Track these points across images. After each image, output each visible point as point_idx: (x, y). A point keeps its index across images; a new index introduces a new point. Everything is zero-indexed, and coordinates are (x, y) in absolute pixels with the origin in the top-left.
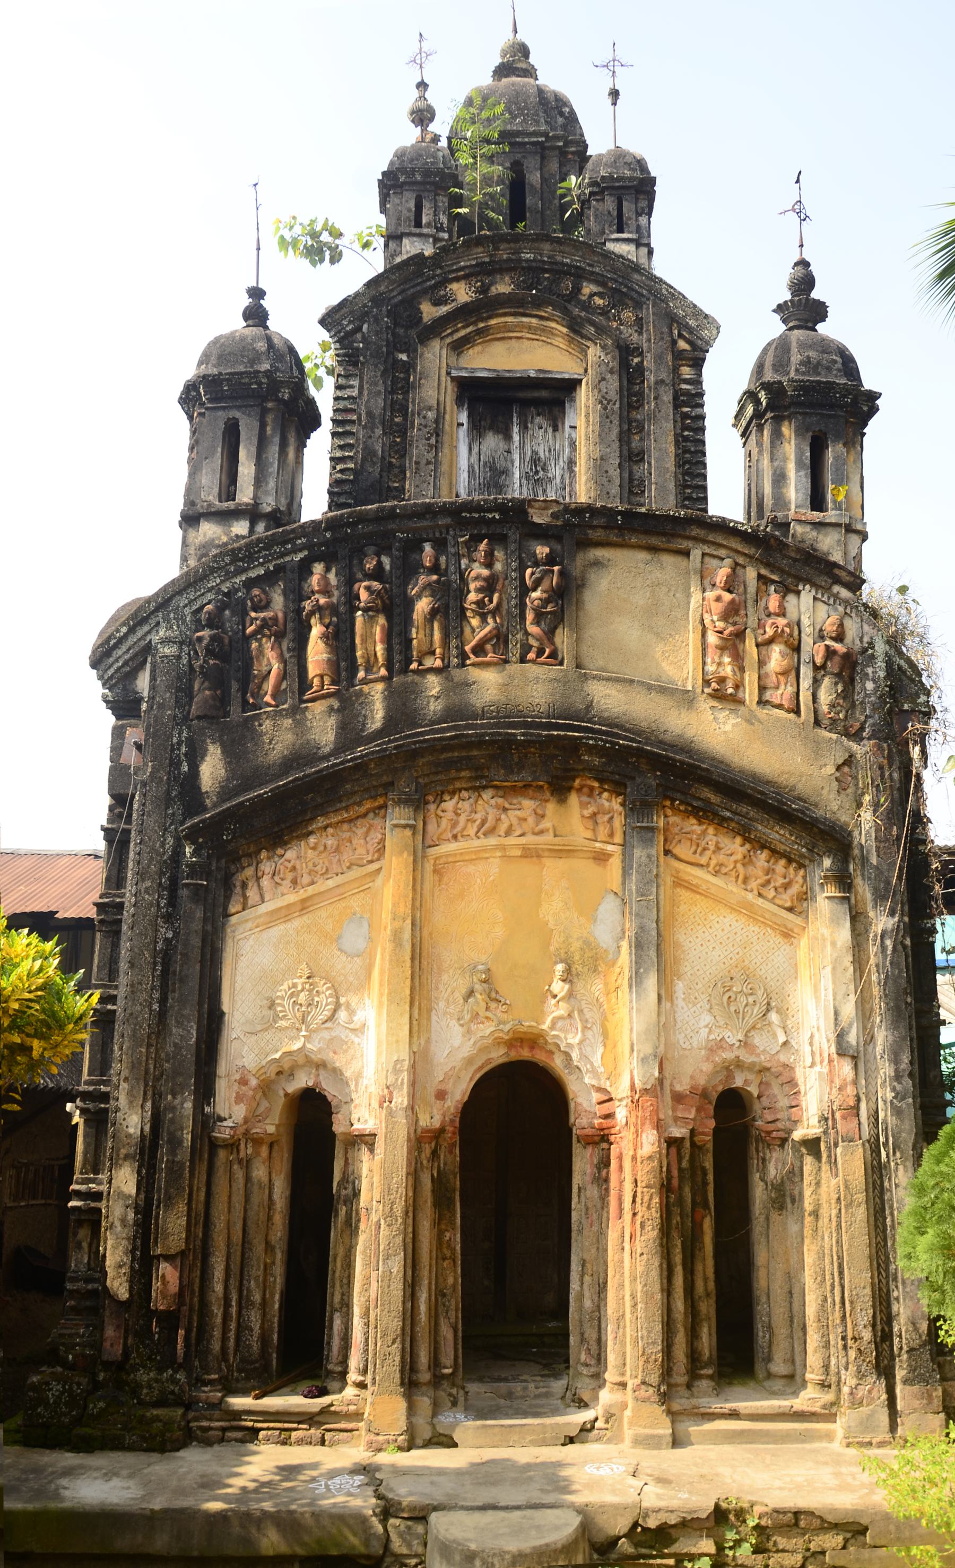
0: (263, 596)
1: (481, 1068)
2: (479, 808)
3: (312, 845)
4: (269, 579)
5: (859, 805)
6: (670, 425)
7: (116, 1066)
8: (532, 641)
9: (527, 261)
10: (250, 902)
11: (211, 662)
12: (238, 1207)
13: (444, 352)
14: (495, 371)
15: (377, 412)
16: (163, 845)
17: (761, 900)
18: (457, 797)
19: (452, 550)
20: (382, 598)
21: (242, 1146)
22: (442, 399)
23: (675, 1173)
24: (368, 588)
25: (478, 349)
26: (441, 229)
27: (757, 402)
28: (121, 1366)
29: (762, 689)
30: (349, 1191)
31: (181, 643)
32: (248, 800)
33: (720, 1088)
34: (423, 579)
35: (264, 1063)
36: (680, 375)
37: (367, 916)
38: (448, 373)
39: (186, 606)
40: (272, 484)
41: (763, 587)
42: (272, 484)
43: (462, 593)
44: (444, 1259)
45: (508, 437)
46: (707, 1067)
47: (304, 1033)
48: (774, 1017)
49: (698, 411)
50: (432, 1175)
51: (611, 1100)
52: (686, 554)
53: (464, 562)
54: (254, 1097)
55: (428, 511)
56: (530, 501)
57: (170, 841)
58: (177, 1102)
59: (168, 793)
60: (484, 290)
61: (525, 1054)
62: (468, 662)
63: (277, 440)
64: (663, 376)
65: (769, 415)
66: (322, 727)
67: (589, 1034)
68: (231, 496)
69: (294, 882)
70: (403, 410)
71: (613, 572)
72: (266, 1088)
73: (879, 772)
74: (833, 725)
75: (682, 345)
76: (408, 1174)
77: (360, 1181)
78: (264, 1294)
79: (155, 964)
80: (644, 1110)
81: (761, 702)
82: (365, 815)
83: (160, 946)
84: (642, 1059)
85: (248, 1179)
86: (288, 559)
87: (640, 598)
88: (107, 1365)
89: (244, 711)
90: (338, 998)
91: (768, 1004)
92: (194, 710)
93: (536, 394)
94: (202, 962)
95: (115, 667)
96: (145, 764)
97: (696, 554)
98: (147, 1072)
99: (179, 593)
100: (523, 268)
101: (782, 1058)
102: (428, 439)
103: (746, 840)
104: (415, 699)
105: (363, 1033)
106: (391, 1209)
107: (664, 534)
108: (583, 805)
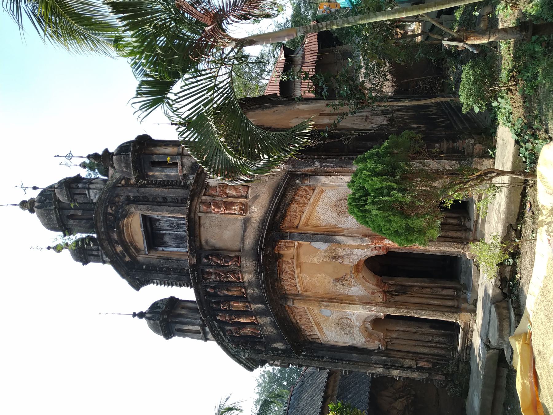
8: (234, 263)
15: (164, 276)
16: (302, 359)
28: (447, 375)
29: (242, 197)
31: (244, 352)
36: (135, 184)
43: (221, 282)
52: (200, 217)
53: (211, 281)
59: (287, 357)
60: (117, 242)
66: (265, 320)
67: (355, 253)
72: (370, 335)
81: (246, 197)
87: (217, 230)
88: (446, 378)
92: (263, 349)
93: (149, 226)
94: (335, 352)
97: (199, 214)
108: (283, 250)
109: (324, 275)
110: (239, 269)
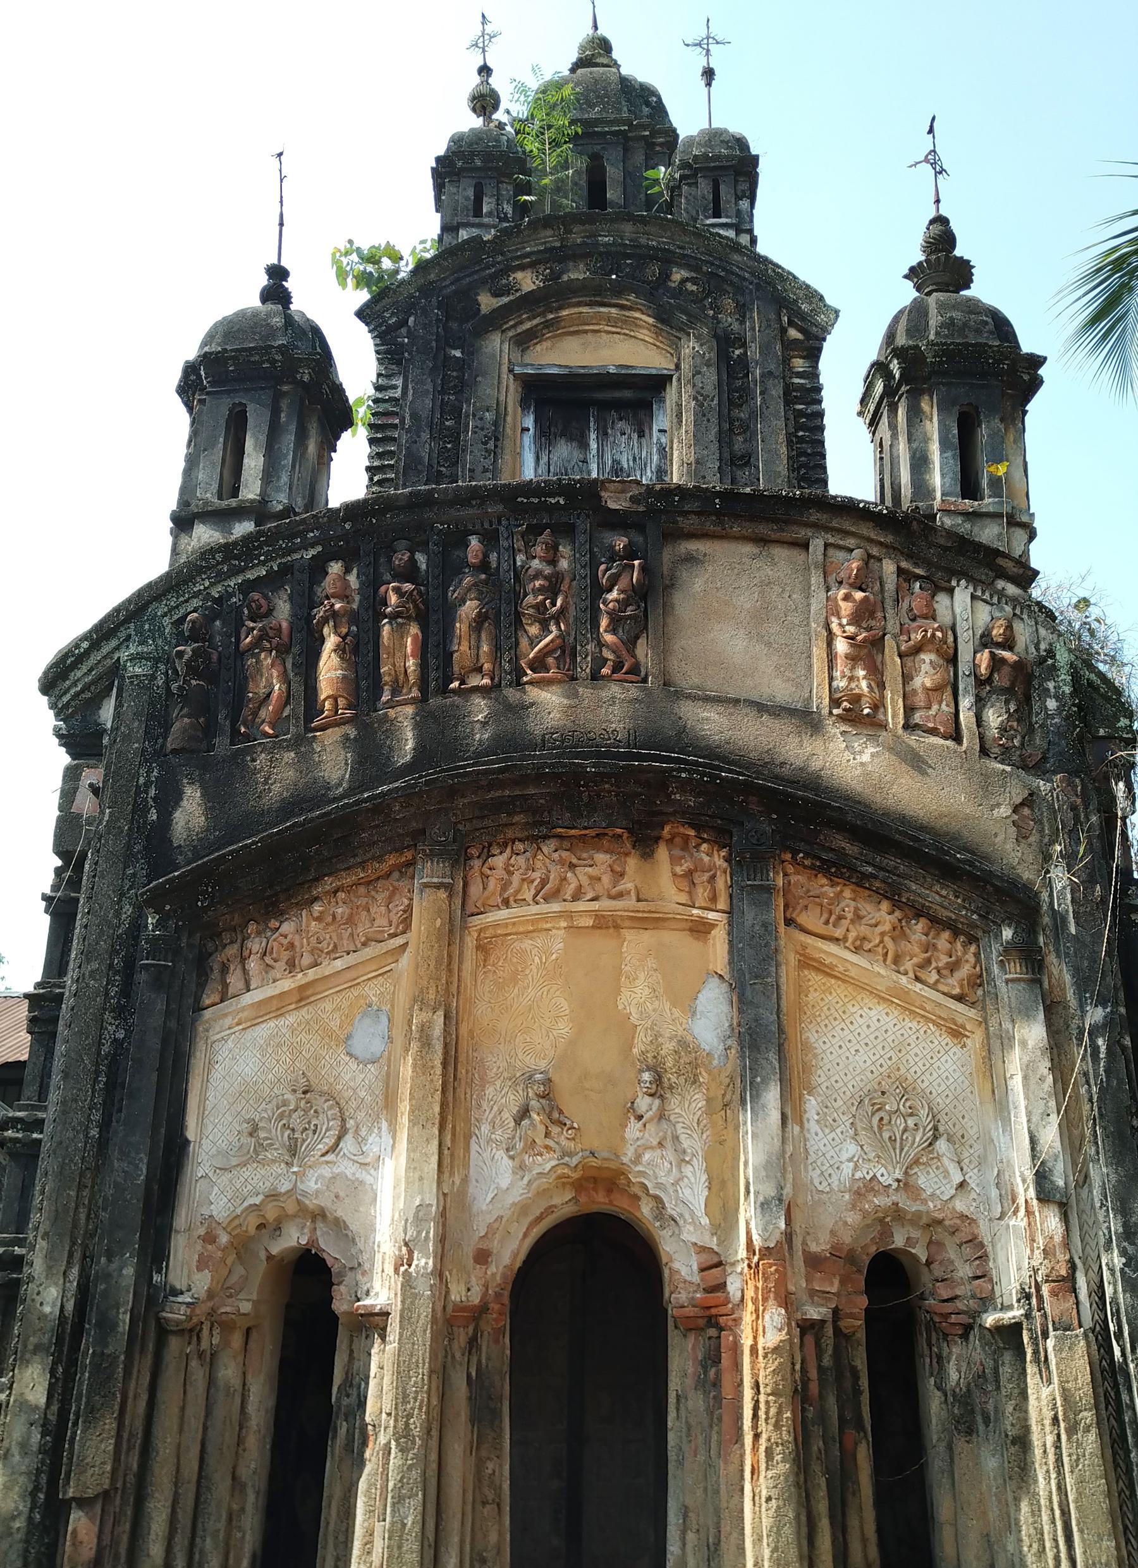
0: (262, 601)
1: (539, 1219)
2: (539, 864)
3: (316, 914)
4: (273, 582)
5: (1047, 858)
6: (781, 423)
7: (35, 1217)
8: (607, 654)
9: (606, 245)
10: (231, 991)
11: (194, 682)
12: (194, 1424)
13: (506, 346)
14: (566, 367)
15: (424, 414)
16: (118, 914)
17: (919, 986)
18: (509, 850)
19: (506, 544)
20: (414, 602)
21: (205, 1332)
22: (502, 398)
23: (813, 1374)
24: (397, 590)
25: (548, 344)
26: (505, 219)
27: (888, 375)
29: (909, 710)
30: (353, 1399)
32: (231, 853)
33: (873, 1250)
34: (467, 580)
35: (239, 1211)
36: (790, 369)
37: (386, 1008)
38: (511, 371)
39: (165, 615)
40: (285, 478)
41: (906, 585)
42: (285, 478)
43: (517, 597)
44: (484, 1503)
45: (584, 446)
46: (852, 1218)
47: (295, 1169)
48: (942, 1145)
49: (815, 407)
50: (469, 1376)
51: (719, 1264)
52: (805, 546)
53: (520, 559)
54: (223, 1260)
55: (476, 496)
56: (603, 482)
57: (128, 909)
58: (113, 1266)
59: (129, 847)
60: (555, 276)
61: (600, 1202)
62: (525, 679)
63: (293, 427)
64: (772, 367)
65: (904, 389)
66: (333, 759)
67: (687, 1170)
68: (235, 492)
69: (292, 965)
70: (457, 413)
71: (710, 569)
72: (242, 1247)
73: (1071, 815)
74: (1005, 755)
75: (793, 333)
76: (431, 1372)
77: (367, 1384)
78: (227, 1559)
79: (97, 1073)
80: (766, 1280)
82: (388, 876)
83: (105, 1049)
84: (762, 1204)
85: (211, 1382)
86: (297, 556)
87: (746, 601)
89: (232, 743)
90: (343, 1120)
91: (936, 1128)
93: (617, 394)
94: (161, 1070)
95: (72, 692)
96: (102, 812)
97: (817, 545)
98: (75, 1224)
99: (157, 598)
100: (601, 254)
101: (960, 1206)
102: (486, 443)
103: (896, 905)
104: (455, 726)
105: (376, 1169)
106: (407, 1424)
107: (775, 521)
109: (564, 1028)
110: (585, 668)
